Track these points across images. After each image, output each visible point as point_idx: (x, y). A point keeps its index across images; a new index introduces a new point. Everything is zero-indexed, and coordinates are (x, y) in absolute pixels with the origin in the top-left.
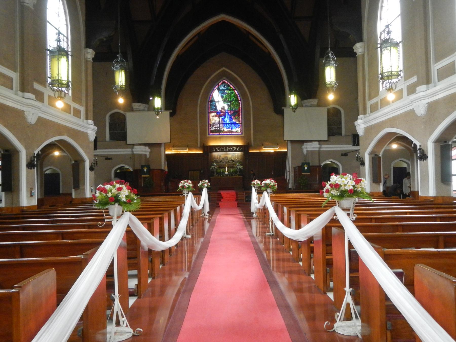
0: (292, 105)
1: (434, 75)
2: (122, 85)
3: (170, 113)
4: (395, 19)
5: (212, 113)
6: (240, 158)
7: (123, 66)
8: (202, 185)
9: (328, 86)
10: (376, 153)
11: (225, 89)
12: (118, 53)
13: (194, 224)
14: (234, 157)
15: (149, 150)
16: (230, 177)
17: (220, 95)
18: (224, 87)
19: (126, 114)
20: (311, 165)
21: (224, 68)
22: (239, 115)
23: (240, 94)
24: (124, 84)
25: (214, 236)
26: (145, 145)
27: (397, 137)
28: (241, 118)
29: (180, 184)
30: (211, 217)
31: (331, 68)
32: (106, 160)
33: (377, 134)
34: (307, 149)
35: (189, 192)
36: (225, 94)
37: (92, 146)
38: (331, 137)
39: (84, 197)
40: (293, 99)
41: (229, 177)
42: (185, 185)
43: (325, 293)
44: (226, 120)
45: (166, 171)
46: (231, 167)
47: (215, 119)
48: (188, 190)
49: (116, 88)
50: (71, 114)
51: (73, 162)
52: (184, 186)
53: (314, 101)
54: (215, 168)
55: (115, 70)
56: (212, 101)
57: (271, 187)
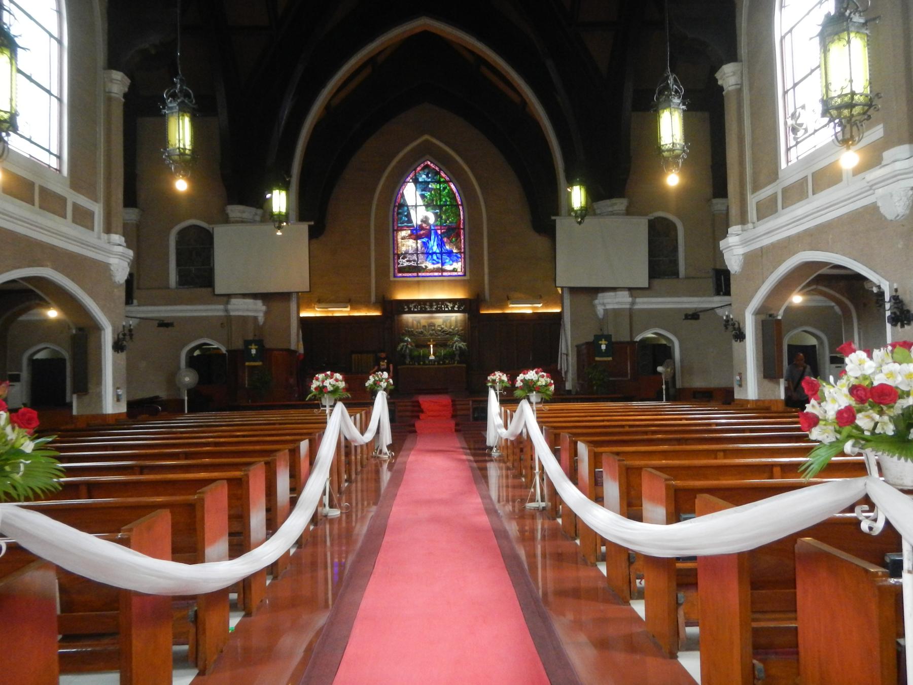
0: (575, 209)
2: (185, 149)
3: (310, 227)
4: (802, 19)
5: (402, 230)
6: (461, 326)
7: (186, 104)
8: (376, 383)
9: (665, 154)
10: (772, 312)
11: (430, 180)
12: (176, 74)
13: (353, 476)
14: (448, 325)
15: (264, 308)
17: (418, 193)
19: (213, 229)
20: (613, 340)
21: (426, 137)
22: (458, 236)
23: (460, 192)
24: (188, 146)
25: (398, 511)
26: (255, 296)
27: (819, 276)
28: (462, 241)
29: (314, 381)
30: (395, 457)
31: (673, 113)
32: (161, 329)
33: (775, 268)
34: (605, 306)
35: (335, 404)
37: (121, 294)
38: (656, 282)
39: (99, 412)
40: (578, 196)
42: (324, 384)
43: (674, 656)
44: (430, 246)
45: (300, 354)
46: (441, 346)
47: (407, 244)
48: (333, 397)
49: (169, 156)
50: (33, 205)
51: (74, 331)
52: (325, 387)
53: (620, 204)
54: (407, 346)
55: (168, 114)
56: (403, 205)
57: (539, 390)
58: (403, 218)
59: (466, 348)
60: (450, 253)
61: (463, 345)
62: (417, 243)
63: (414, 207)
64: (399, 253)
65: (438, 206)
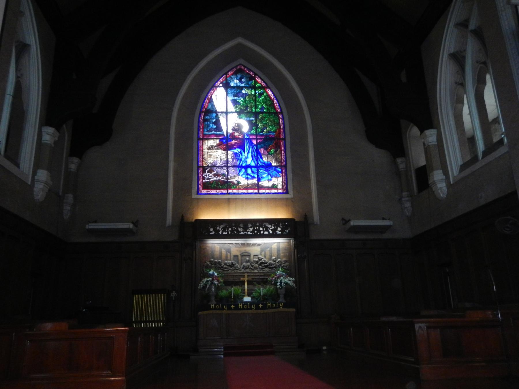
5: (208, 139)
6: (284, 256)
11: (243, 85)
14: (268, 254)
16: (259, 311)
17: (230, 98)
18: (240, 80)
23: (279, 98)
28: (283, 152)
36: (242, 97)
41: (255, 311)
44: (244, 158)
46: (259, 283)
54: (212, 283)
56: (211, 111)
58: (211, 125)
59: (294, 285)
60: (268, 167)
61: (290, 280)
62: (227, 154)
63: (224, 114)
64: (204, 165)
65: (253, 112)
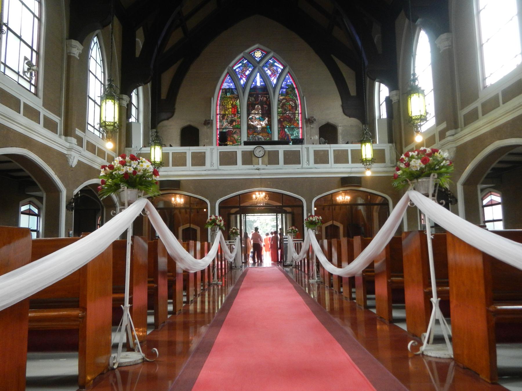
1: (461, 120)
